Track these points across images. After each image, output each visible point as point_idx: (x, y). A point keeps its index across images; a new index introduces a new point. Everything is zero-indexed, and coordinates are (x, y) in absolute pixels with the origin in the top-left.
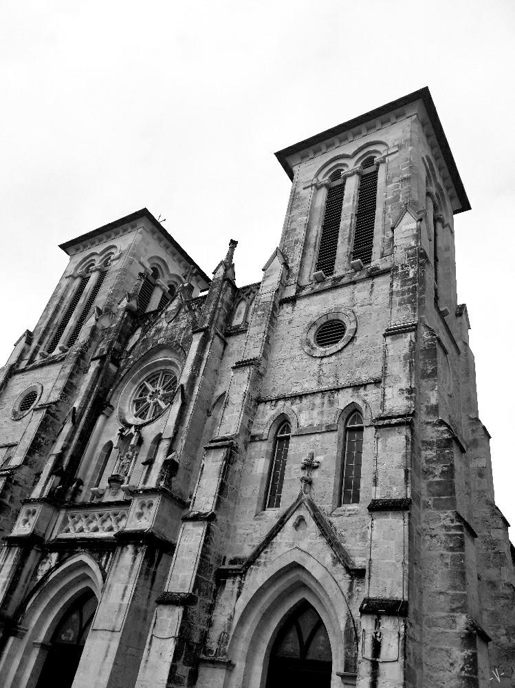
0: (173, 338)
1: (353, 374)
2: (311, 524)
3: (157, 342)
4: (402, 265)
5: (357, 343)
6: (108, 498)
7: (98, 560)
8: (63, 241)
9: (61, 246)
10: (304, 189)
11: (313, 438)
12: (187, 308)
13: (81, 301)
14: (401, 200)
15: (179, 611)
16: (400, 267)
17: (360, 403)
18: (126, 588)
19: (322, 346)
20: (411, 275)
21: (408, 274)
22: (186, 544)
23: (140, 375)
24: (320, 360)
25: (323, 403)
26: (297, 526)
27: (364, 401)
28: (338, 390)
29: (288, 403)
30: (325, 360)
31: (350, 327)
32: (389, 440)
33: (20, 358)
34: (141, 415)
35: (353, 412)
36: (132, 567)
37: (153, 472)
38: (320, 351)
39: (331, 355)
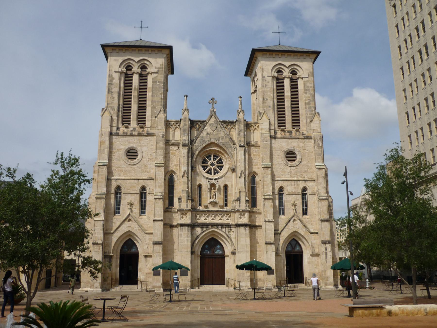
0: (219, 140)
1: (302, 175)
2: (298, 221)
3: (210, 140)
4: (317, 140)
5: (302, 163)
6: (211, 208)
7: (221, 230)
8: (105, 42)
9: (104, 47)
10: (268, 76)
11: (293, 196)
12: (222, 126)
13: (135, 94)
14: (311, 105)
15: (273, 246)
16: (317, 141)
17: (307, 187)
18: (246, 240)
19: (288, 161)
20: (320, 145)
21: (319, 144)
22: (268, 228)
23: (203, 154)
24: (290, 167)
25: (295, 185)
26: (293, 221)
27: (309, 186)
28: (299, 181)
29: (282, 182)
30: (292, 168)
31: (298, 157)
32: (323, 203)
33: (111, 126)
34: (209, 172)
35: (304, 189)
36: (246, 234)
37: (241, 203)
38: (290, 163)
39: (294, 167)
